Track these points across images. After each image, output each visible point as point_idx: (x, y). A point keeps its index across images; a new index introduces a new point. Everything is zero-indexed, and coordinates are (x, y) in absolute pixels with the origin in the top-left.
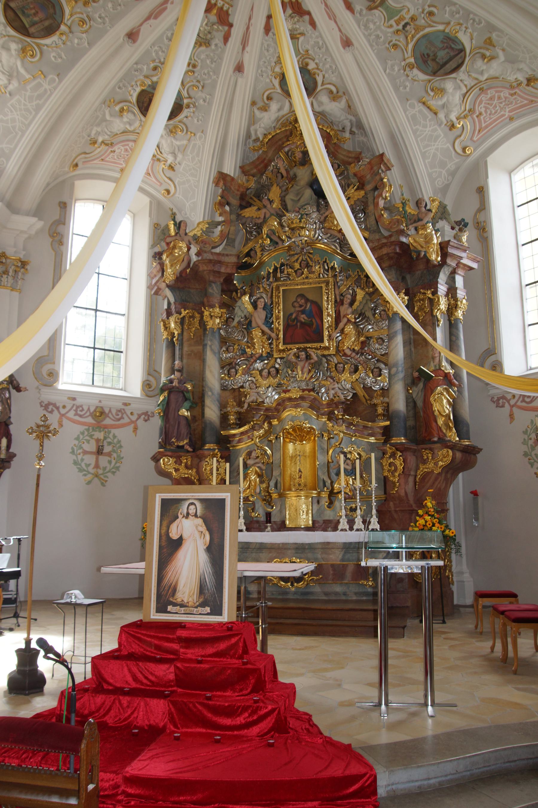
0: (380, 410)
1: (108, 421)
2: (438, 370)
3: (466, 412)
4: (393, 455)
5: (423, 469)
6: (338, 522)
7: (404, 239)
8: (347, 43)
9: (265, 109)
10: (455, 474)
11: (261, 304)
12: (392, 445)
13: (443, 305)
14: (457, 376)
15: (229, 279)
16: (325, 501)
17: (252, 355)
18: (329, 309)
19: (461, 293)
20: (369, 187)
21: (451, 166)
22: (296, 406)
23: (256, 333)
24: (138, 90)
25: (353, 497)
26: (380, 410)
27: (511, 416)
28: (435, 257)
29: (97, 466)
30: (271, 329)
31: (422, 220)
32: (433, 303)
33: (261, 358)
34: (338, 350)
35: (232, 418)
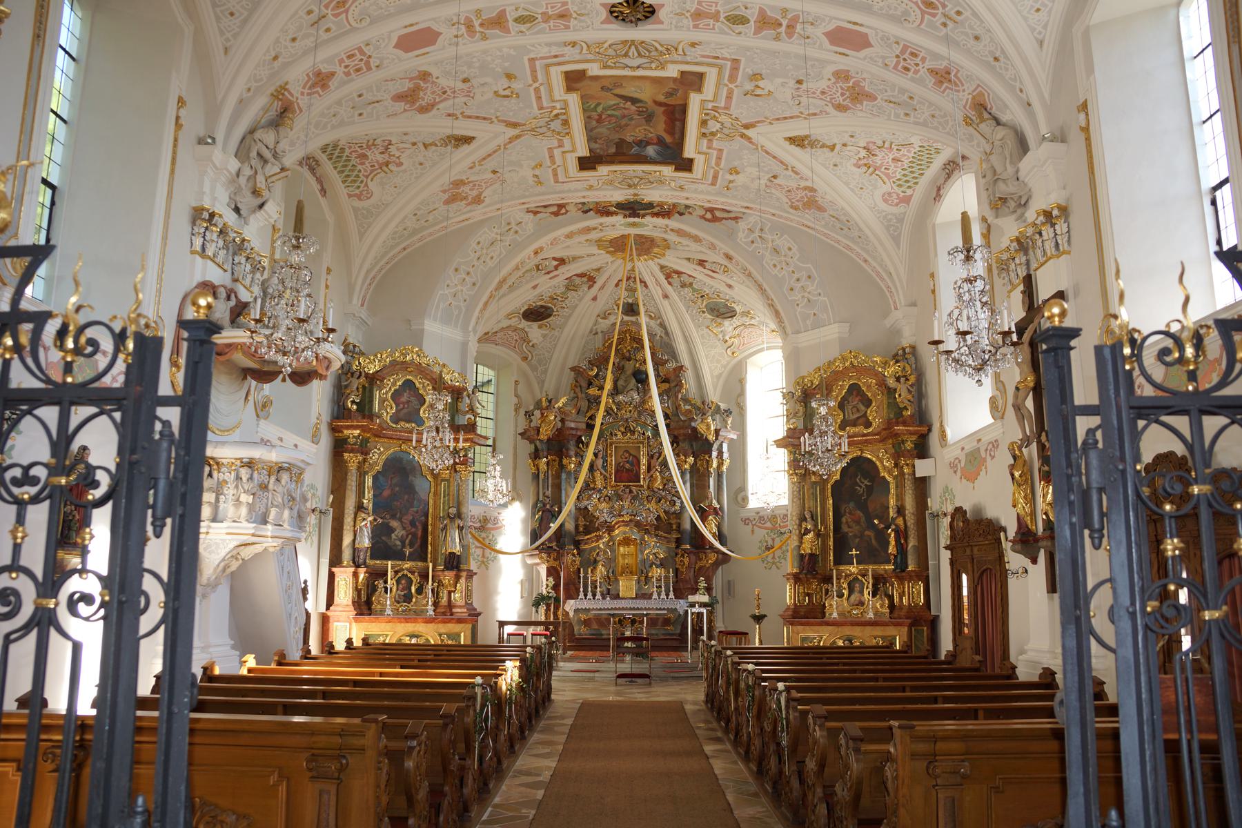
0: (674, 527)
1: (489, 526)
2: (710, 506)
3: (725, 530)
4: (683, 556)
5: (700, 564)
6: (652, 594)
7: (693, 424)
8: (666, 296)
9: (604, 318)
10: (717, 568)
11: (600, 455)
12: (683, 550)
13: (715, 465)
14: (721, 509)
15: (580, 437)
16: (643, 583)
17: (594, 489)
18: (644, 461)
19: (726, 455)
20: (673, 385)
21: (724, 362)
22: (627, 526)
23: (597, 474)
24: (526, 307)
25: (660, 580)
26: (674, 527)
27: (753, 531)
28: (711, 438)
29: (483, 556)
30: (606, 471)
31: (704, 414)
32: (709, 463)
33: (600, 491)
34: (649, 488)
35: (581, 529)
